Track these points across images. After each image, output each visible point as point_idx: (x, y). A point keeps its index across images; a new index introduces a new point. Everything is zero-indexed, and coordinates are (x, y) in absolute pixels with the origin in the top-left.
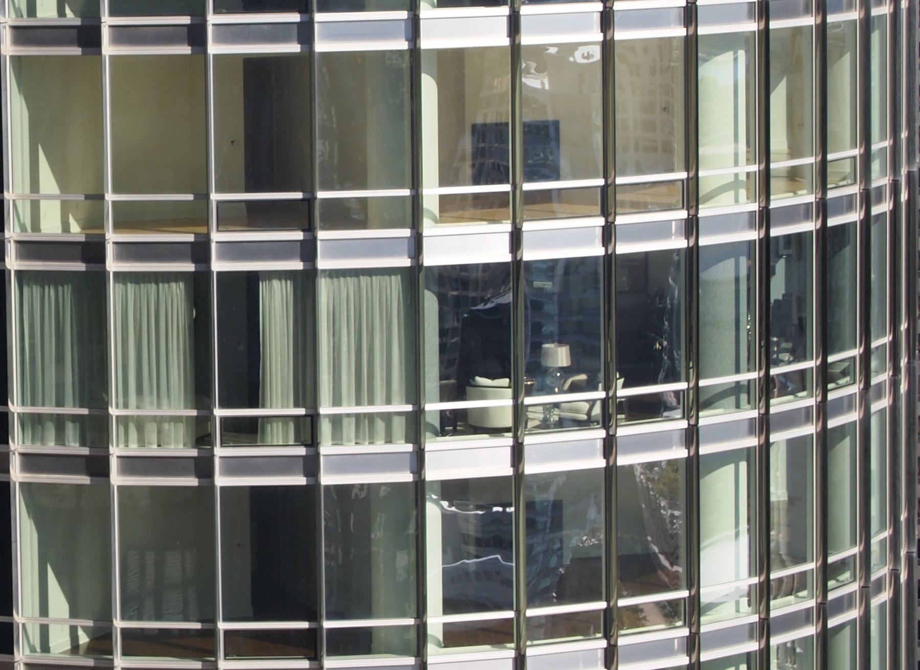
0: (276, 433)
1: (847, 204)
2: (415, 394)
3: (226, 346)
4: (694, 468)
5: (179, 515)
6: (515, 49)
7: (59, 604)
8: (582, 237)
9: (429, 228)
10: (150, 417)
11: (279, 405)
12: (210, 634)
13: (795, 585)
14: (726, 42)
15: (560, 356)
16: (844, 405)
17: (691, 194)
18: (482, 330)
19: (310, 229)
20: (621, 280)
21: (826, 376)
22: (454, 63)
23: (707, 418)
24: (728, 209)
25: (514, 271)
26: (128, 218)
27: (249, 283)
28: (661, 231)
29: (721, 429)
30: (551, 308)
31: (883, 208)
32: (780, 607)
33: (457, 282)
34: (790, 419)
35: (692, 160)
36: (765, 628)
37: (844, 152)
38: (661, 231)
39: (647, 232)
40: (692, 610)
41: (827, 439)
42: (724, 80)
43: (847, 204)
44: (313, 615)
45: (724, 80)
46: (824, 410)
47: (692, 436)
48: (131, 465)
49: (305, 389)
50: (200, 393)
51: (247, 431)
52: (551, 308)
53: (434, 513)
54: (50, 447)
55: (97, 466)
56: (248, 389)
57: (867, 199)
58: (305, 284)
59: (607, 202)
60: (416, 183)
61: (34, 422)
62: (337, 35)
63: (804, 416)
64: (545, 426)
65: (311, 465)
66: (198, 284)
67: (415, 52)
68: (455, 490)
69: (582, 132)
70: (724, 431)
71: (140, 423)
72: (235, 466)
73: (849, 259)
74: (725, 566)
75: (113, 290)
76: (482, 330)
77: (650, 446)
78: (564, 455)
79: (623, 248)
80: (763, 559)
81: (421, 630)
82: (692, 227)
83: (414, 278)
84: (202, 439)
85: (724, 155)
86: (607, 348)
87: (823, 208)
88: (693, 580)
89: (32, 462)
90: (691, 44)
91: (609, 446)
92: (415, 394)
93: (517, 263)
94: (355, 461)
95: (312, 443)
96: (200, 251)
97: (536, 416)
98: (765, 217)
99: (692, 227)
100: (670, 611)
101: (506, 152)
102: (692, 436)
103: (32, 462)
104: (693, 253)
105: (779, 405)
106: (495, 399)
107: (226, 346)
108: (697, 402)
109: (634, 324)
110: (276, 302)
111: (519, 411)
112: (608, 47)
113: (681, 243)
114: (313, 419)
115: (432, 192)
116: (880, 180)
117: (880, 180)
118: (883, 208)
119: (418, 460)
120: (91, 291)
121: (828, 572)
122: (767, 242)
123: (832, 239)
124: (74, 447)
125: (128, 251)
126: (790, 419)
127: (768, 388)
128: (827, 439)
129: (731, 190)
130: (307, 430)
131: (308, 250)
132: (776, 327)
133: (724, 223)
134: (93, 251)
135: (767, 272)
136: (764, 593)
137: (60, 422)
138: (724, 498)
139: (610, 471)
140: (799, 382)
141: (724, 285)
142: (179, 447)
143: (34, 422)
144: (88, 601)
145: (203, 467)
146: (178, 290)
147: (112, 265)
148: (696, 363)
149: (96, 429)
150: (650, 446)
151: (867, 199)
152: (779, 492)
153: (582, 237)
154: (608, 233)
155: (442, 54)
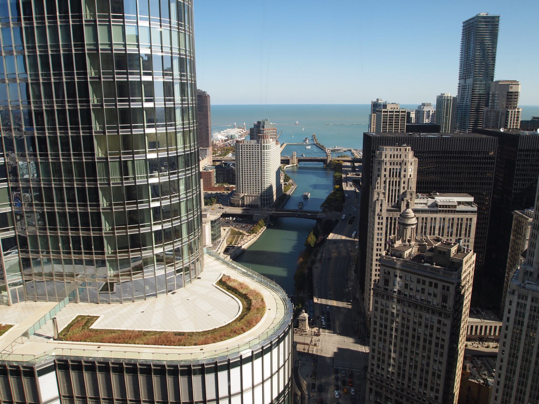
0: (131, 179)
2: (147, 174)
3: (124, 169)
4: (178, 180)
5: (118, 190)
10: (115, 178)
11: (131, 176)
12: (124, 203)
14: (179, 132)
18: (154, 166)
19: (133, 155)
21: (192, 169)
23: (180, 174)
26: (110, 154)
27: (126, 162)
32: (188, 195)
39: (172, 154)
42: (179, 136)
44: (136, 200)
45: (179, 136)
46: (192, 173)
48: (113, 184)
49: (134, 173)
50: (121, 175)
51: (127, 179)
54: (103, 182)
55: (109, 184)
56: (127, 174)
57: (195, 149)
58: (133, 161)
59: (168, 150)
60: (146, 149)
61: (100, 180)
62: (135, 132)
63: (189, 173)
65: (135, 182)
66: (120, 162)
67: (145, 133)
70: (182, 176)
71: (114, 179)
72: (126, 183)
75: (109, 163)
76: (154, 166)
77: (174, 178)
81: (149, 200)
83: (146, 160)
84: (121, 180)
85: (180, 145)
87: (190, 150)
89: (100, 184)
90: (176, 132)
92: (147, 174)
93: (158, 158)
94: (140, 182)
95: (135, 180)
96: (120, 158)
99: (177, 153)
101: (154, 145)
102: (178, 176)
103: (100, 184)
105: (187, 172)
107: (124, 169)
108: (179, 172)
110: (130, 164)
111: (159, 174)
114: (135, 177)
115: (147, 150)
119: (148, 181)
120: (107, 163)
123: (191, 153)
124: (106, 182)
125: (111, 158)
127: (186, 171)
128: (192, 175)
130: (134, 178)
131: (133, 157)
133: (180, 152)
134: (107, 158)
136: (186, 193)
137: (104, 179)
139: (170, 181)
140: (188, 170)
142: (119, 181)
143: (100, 180)
144: (109, 200)
145: (122, 183)
146: (117, 163)
147: (109, 160)
148: (178, 168)
149: (108, 180)
150: (174, 178)
151: (195, 149)
154: (168, 154)
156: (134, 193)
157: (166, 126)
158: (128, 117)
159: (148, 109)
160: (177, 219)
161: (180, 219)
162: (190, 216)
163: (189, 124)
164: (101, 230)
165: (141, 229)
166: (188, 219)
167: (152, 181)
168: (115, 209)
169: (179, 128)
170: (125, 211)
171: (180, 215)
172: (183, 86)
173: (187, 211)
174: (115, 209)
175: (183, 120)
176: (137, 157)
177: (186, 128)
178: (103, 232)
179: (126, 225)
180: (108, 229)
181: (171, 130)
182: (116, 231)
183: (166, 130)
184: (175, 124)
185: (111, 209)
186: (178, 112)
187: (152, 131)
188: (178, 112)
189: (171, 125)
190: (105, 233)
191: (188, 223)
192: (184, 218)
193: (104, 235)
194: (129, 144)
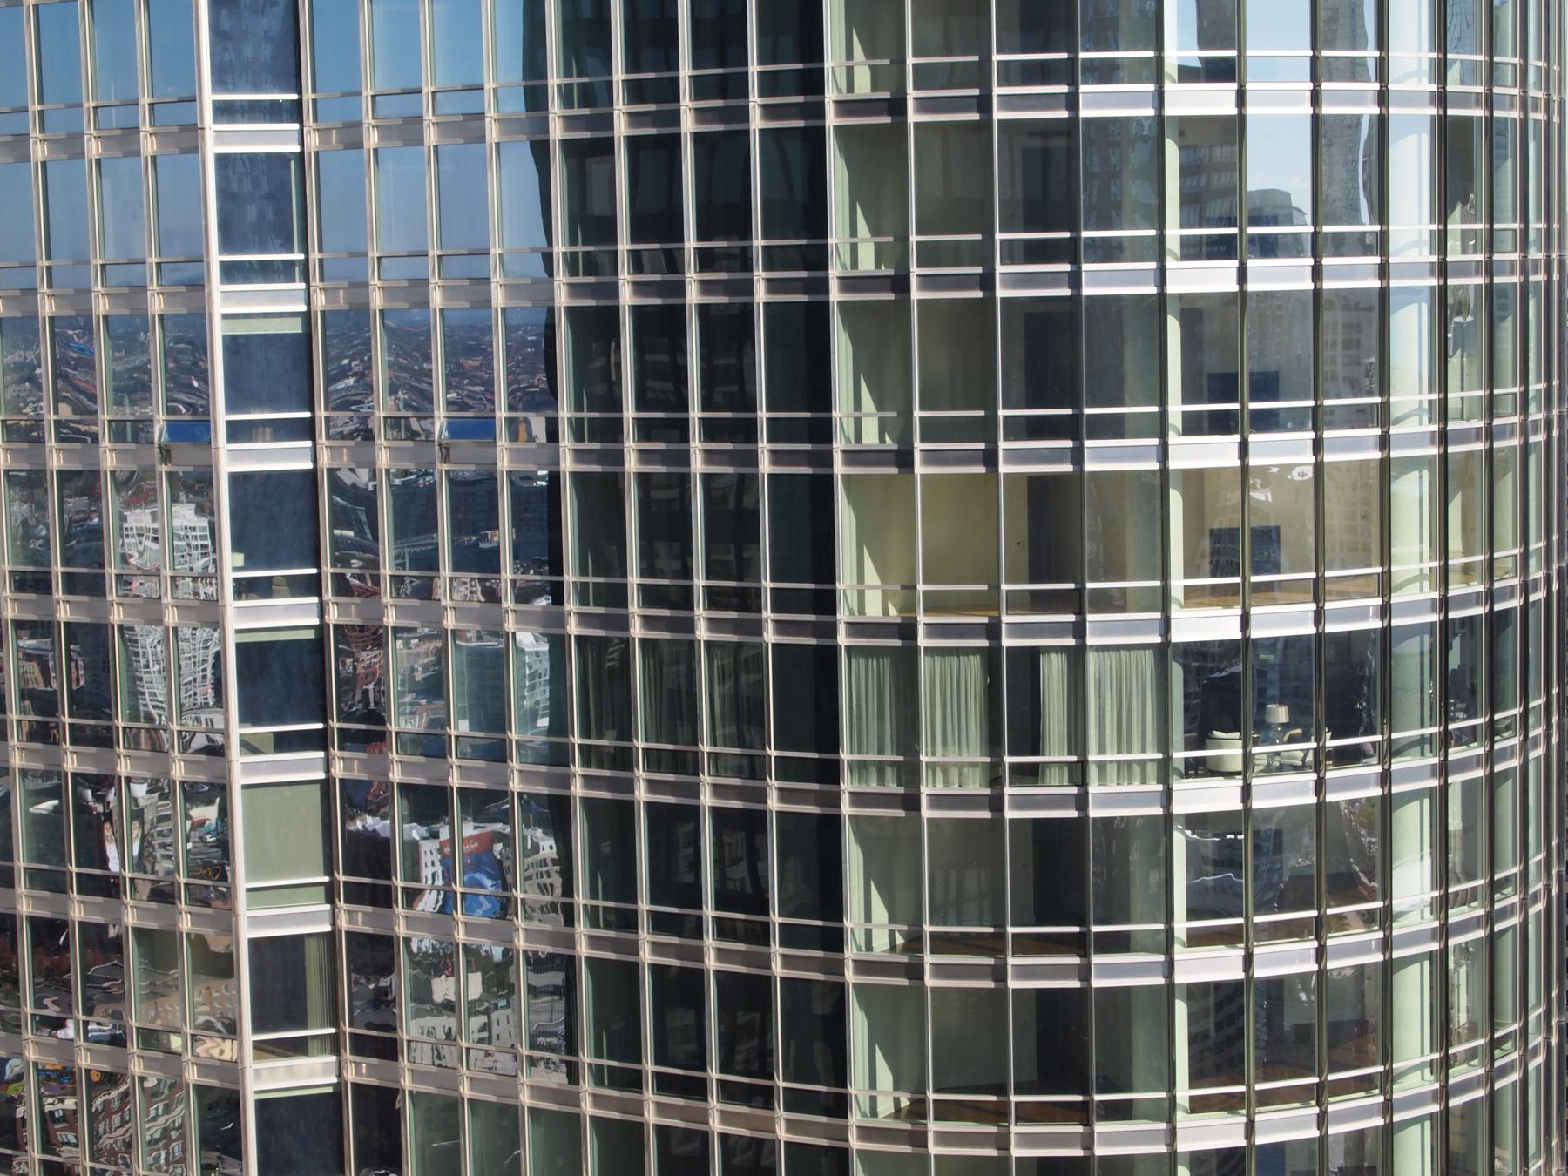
0: (1054, 776)
1: (1509, 593)
2: (1164, 744)
3: (1013, 707)
4: (1387, 805)
5: (976, 842)
6: (1245, 469)
7: (880, 912)
8: (1298, 619)
9: (1175, 612)
10: (953, 763)
11: (1056, 753)
12: (1001, 936)
13: (1468, 898)
14: (1413, 464)
15: (1281, 714)
16: (1507, 753)
17: (1385, 585)
18: (1217, 692)
19: (1080, 612)
20: (1329, 653)
21: (1493, 730)
22: (1196, 481)
23: (1398, 764)
24: (1415, 599)
25: (1243, 647)
26: (935, 604)
27: (1032, 657)
28: (1361, 614)
29: (1409, 773)
30: (1274, 676)
31: (1538, 596)
32: (1457, 915)
33: (1199, 656)
34: (1464, 765)
35: (1386, 557)
36: (1444, 932)
37: (1508, 552)
38: (1361, 614)
39: (1353, 615)
40: (1386, 917)
41: (1493, 781)
43: (1509, 593)
44: (1083, 922)
46: (1491, 757)
47: (1386, 778)
48: (938, 801)
49: (1077, 741)
50: (993, 743)
51: (1030, 774)
52: (1274, 676)
53: (1179, 840)
54: (873, 787)
55: (910, 802)
56: (1031, 740)
57: (1526, 588)
58: (1076, 657)
59: (1318, 591)
60: (1165, 576)
61: (860, 767)
62: (1103, 457)
63: (1474, 762)
64: (1268, 770)
65: (1081, 802)
66: (991, 657)
67: (1164, 471)
68: (1196, 822)
69: (1298, 535)
71: (945, 768)
73: (1512, 636)
74: (1412, 883)
75: (924, 662)
77: (1353, 786)
78: (1284, 793)
79: (1330, 628)
80: (1442, 876)
81: (1170, 932)
82: (1385, 611)
83: (1163, 652)
84: (995, 780)
85: (1411, 555)
86: (1318, 708)
87: (1491, 596)
88: (1386, 893)
89: (858, 799)
90: (1386, 467)
91: (1320, 786)
92: (1164, 744)
93: (1246, 640)
94: (1114, 798)
95: (1082, 783)
96: (993, 630)
97: (1261, 762)
98: (1444, 603)
99: (1385, 611)
100: (1368, 919)
101: (1238, 551)
102: (1386, 778)
103: (858, 799)
104: (1386, 632)
105: (1456, 753)
106: (1229, 749)
107: (1013, 707)
108: (1390, 751)
109: (1339, 689)
110: (1053, 672)
111: (1247, 758)
112: (1318, 467)
113: (1377, 624)
115: (1178, 583)
116: (1536, 573)
117: (1536, 573)
118: (1538, 596)
119: (1167, 796)
120: (905, 662)
121: (1494, 887)
122: (1445, 623)
123: (1497, 621)
124: (892, 787)
125: (935, 630)
126: (1464, 765)
127: (1446, 740)
129: (1416, 582)
130: (1079, 772)
131: (1079, 630)
132: (1453, 692)
134: (907, 630)
135: (1446, 647)
136: (1443, 904)
137: (881, 766)
138: (1412, 825)
139: (1321, 806)
140: (1471, 735)
141: (1411, 658)
143: (860, 767)
144: (904, 910)
145: (996, 803)
146: (975, 662)
147: (923, 642)
149: (910, 772)
150: (1353, 786)
151: (1526, 588)
152: (1455, 823)
153: (1298, 619)
154: (1319, 617)
155: (1186, 473)
156: (1068, 874)
157: (1317, 419)
158: (1063, 360)
159: (1195, 311)
160: (1364, 1084)
161: (1386, 1090)
162: (1458, 1075)
163: (1491, 406)
164: (839, 1107)
165: (1100, 1127)
166: (1445, 1093)
167: (1196, 796)
168: (940, 970)
169: (1413, 440)
170: (1001, 992)
171: (1387, 1056)
172: (1452, 143)
173: (1443, 1033)
174: (940, 970)
175: (1440, 380)
176: (1102, 629)
177: (1464, 436)
178: (855, 1119)
179: (1001, 1090)
180: (885, 1107)
181: (1352, 447)
182: (933, 1126)
183: (1318, 446)
184: (1385, 407)
185: (915, 971)
186: (1410, 331)
187: (1218, 452)
188: (1410, 331)
189: (1359, 417)
190: (866, 1133)
191: (1443, 1121)
192: (1415, 1083)
193: (855, 1143)
194: (1059, 537)
